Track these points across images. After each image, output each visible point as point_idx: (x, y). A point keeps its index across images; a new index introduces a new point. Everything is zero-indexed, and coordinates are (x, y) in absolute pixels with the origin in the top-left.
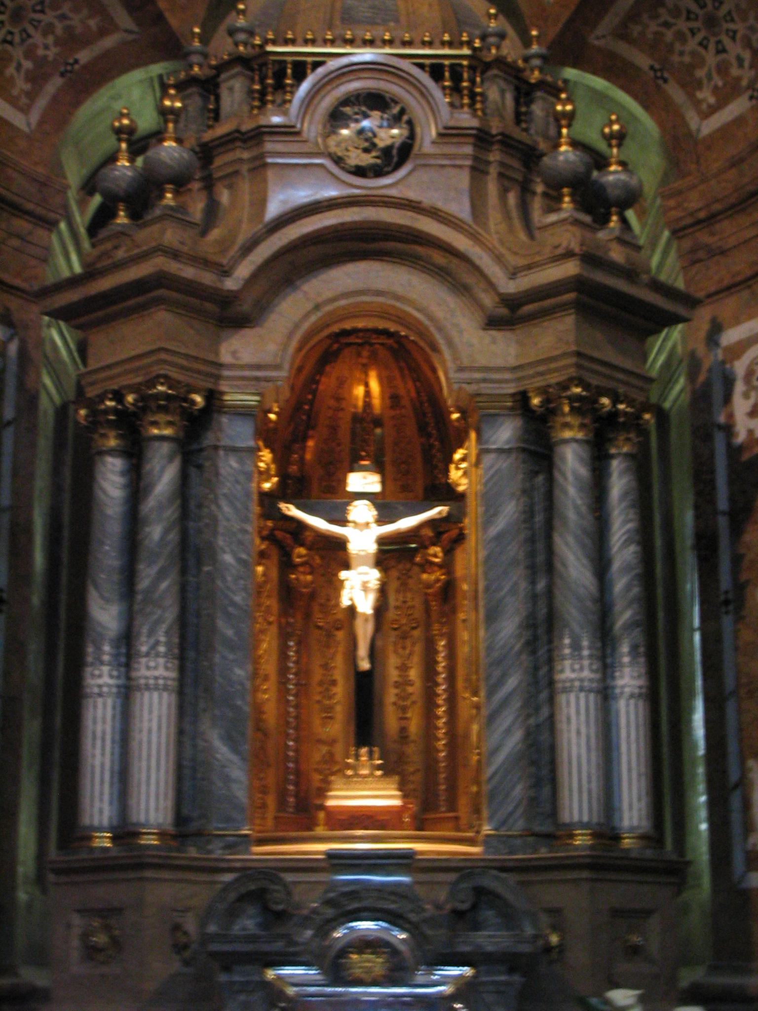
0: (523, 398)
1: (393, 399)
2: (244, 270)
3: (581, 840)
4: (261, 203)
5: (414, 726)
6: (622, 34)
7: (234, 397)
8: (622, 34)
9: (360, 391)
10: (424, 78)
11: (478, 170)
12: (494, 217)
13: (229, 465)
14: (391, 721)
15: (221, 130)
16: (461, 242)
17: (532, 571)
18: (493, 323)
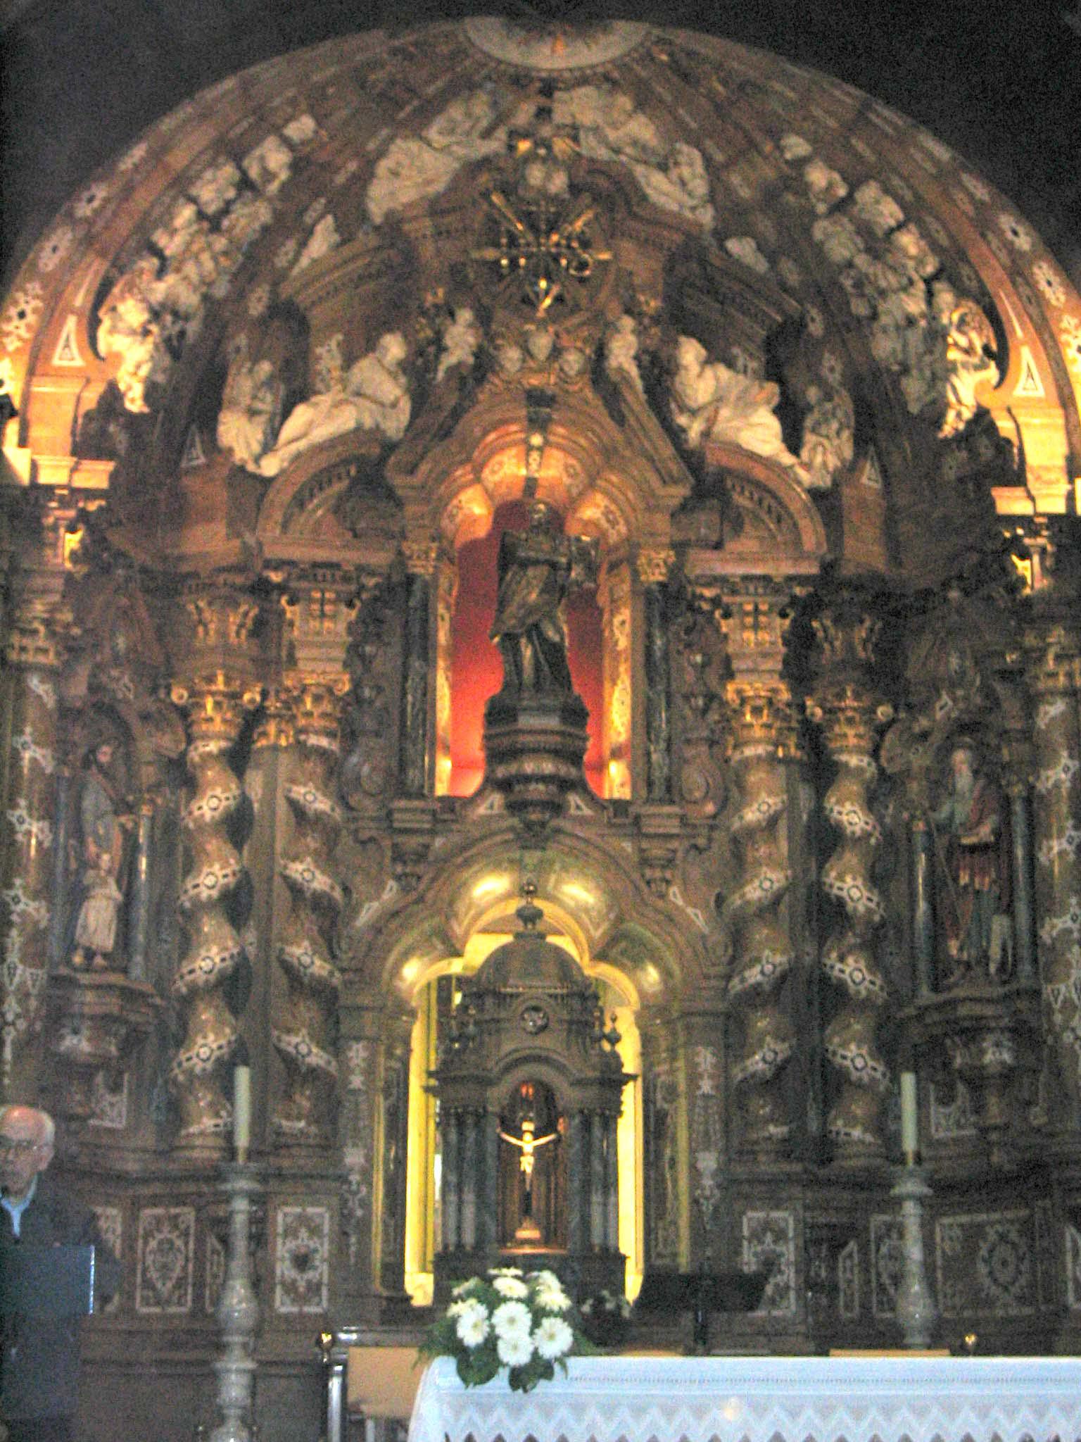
0: (581, 1112)
1: (536, 1092)
2: (496, 1070)
3: (597, 1249)
4: (498, 1045)
5: (543, 1207)
6: (622, 953)
7: (490, 1109)
8: (622, 953)
9: (524, 1090)
10: (552, 1002)
11: (569, 1032)
12: (574, 1050)
13: (489, 1130)
14: (534, 1204)
15: (487, 1017)
16: (562, 1060)
17: (584, 1166)
18: (572, 1084)
